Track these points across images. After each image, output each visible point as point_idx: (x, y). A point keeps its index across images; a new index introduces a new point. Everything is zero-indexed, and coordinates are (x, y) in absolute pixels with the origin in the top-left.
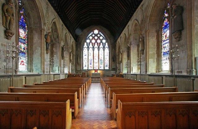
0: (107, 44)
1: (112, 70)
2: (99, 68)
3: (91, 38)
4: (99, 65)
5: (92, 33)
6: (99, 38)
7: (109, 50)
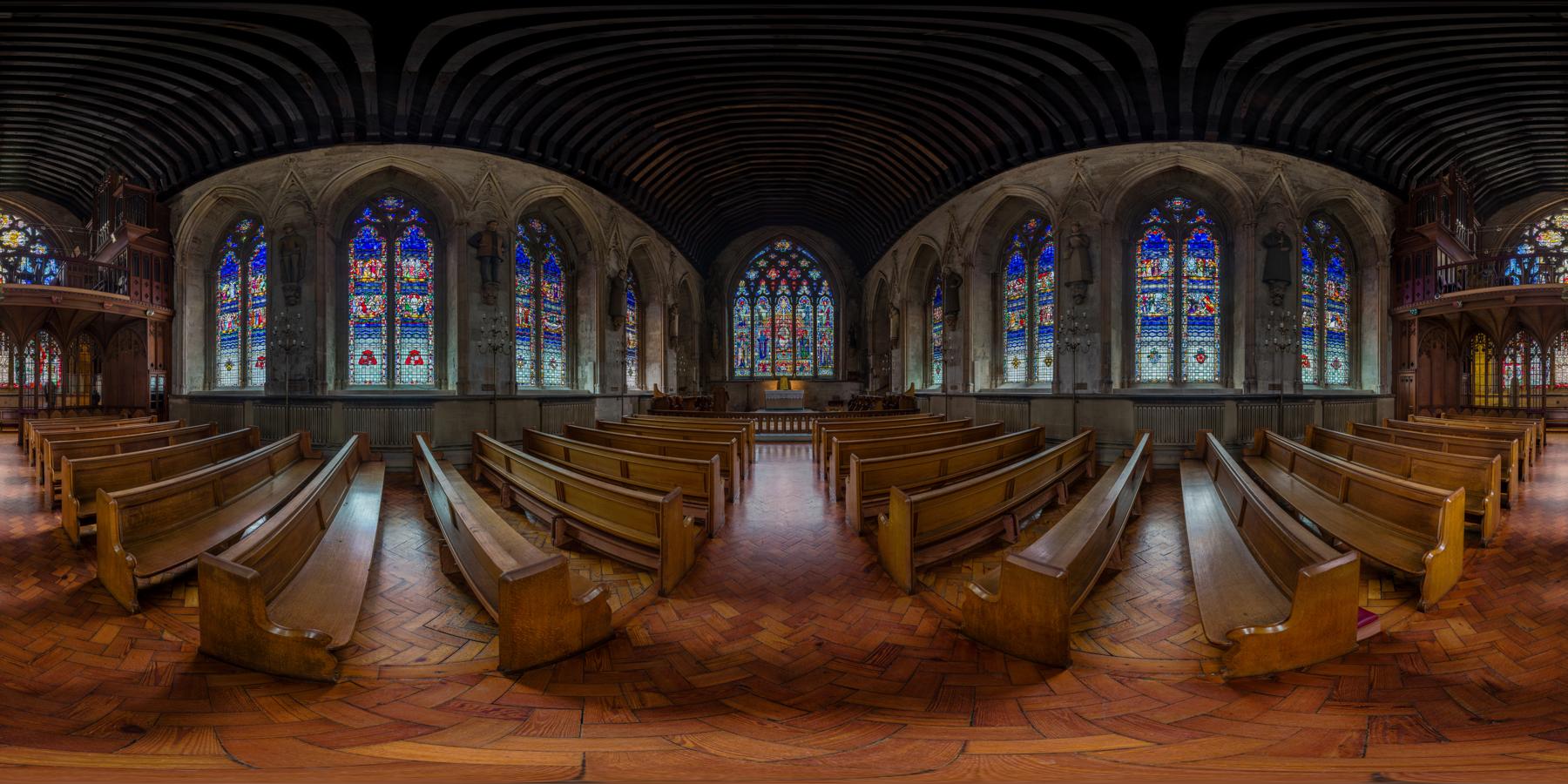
0: (825, 283)
1: (849, 380)
2: (795, 371)
3: (762, 263)
5: (767, 249)
6: (794, 264)
7: (836, 306)
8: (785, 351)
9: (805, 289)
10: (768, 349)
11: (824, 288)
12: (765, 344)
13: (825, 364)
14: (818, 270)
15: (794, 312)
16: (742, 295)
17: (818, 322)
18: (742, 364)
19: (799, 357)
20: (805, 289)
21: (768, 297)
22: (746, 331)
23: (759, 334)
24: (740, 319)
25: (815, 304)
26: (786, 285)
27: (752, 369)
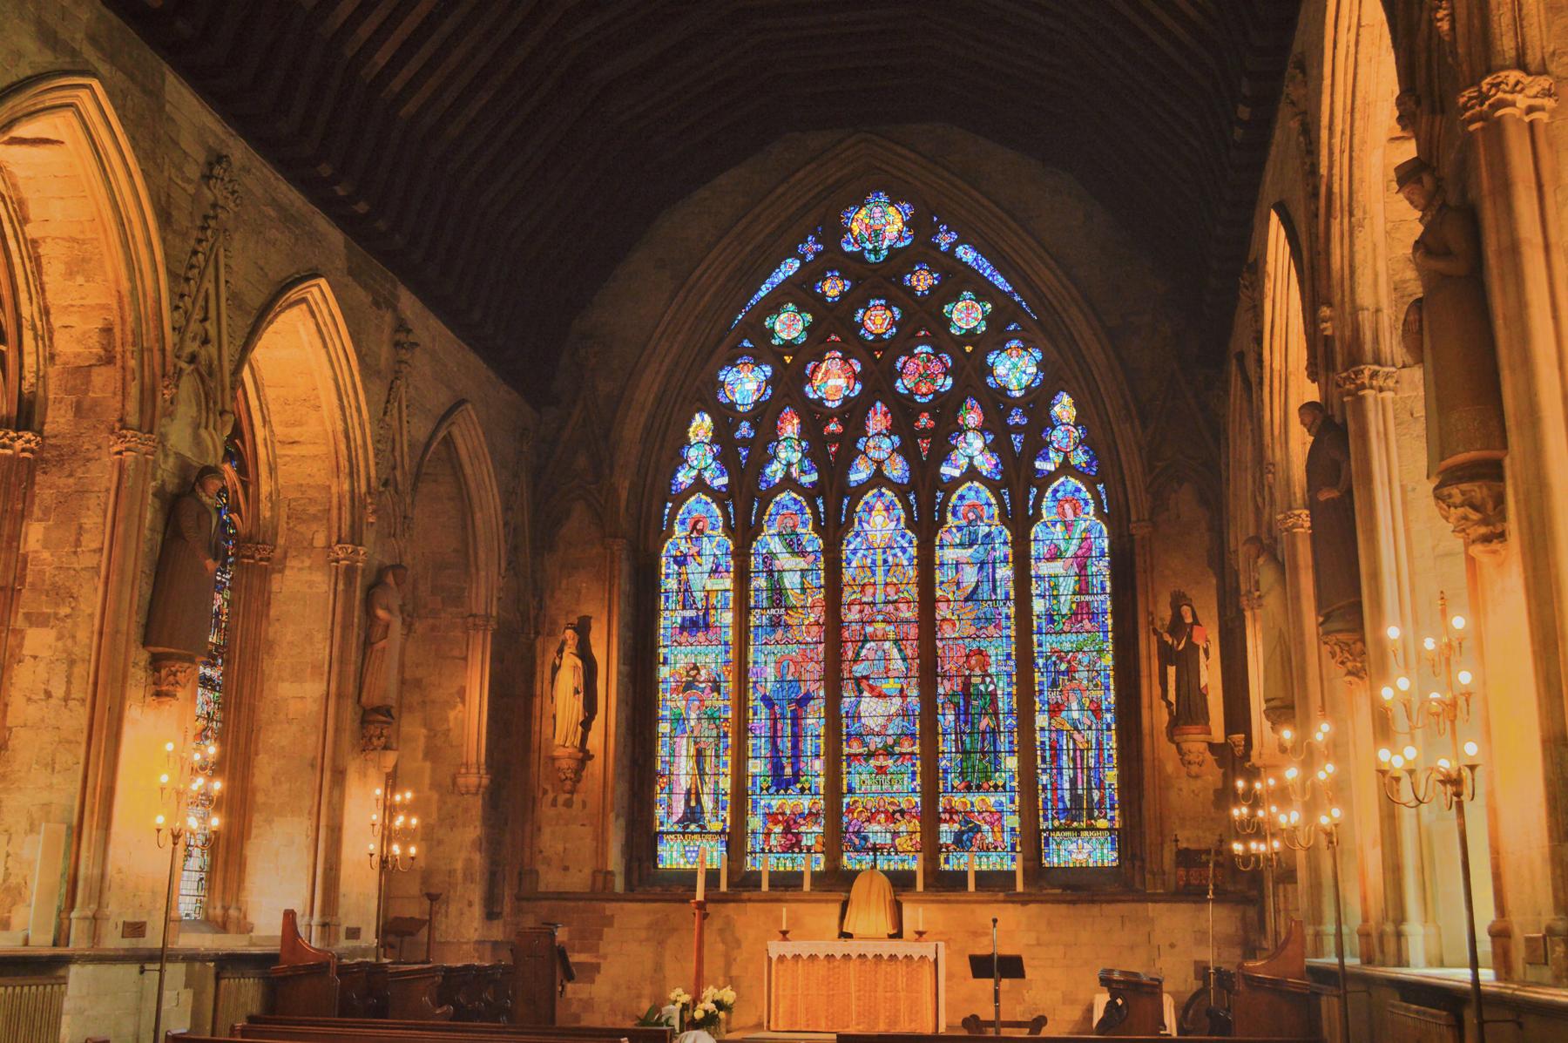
0: (1064, 408)
3: (789, 326)
4: (930, 792)
5: (811, 247)
7: (1115, 517)
8: (888, 752)
9: (973, 449)
10: (808, 746)
11: (1058, 434)
12: (796, 720)
13: (1077, 814)
14: (1027, 345)
15: (926, 565)
16: (699, 485)
17: (1038, 606)
18: (693, 814)
19: (953, 779)
20: (973, 449)
21: (810, 493)
22: (711, 657)
23: (770, 673)
24: (686, 601)
25: (1020, 521)
26: (891, 431)
27: (735, 841)
